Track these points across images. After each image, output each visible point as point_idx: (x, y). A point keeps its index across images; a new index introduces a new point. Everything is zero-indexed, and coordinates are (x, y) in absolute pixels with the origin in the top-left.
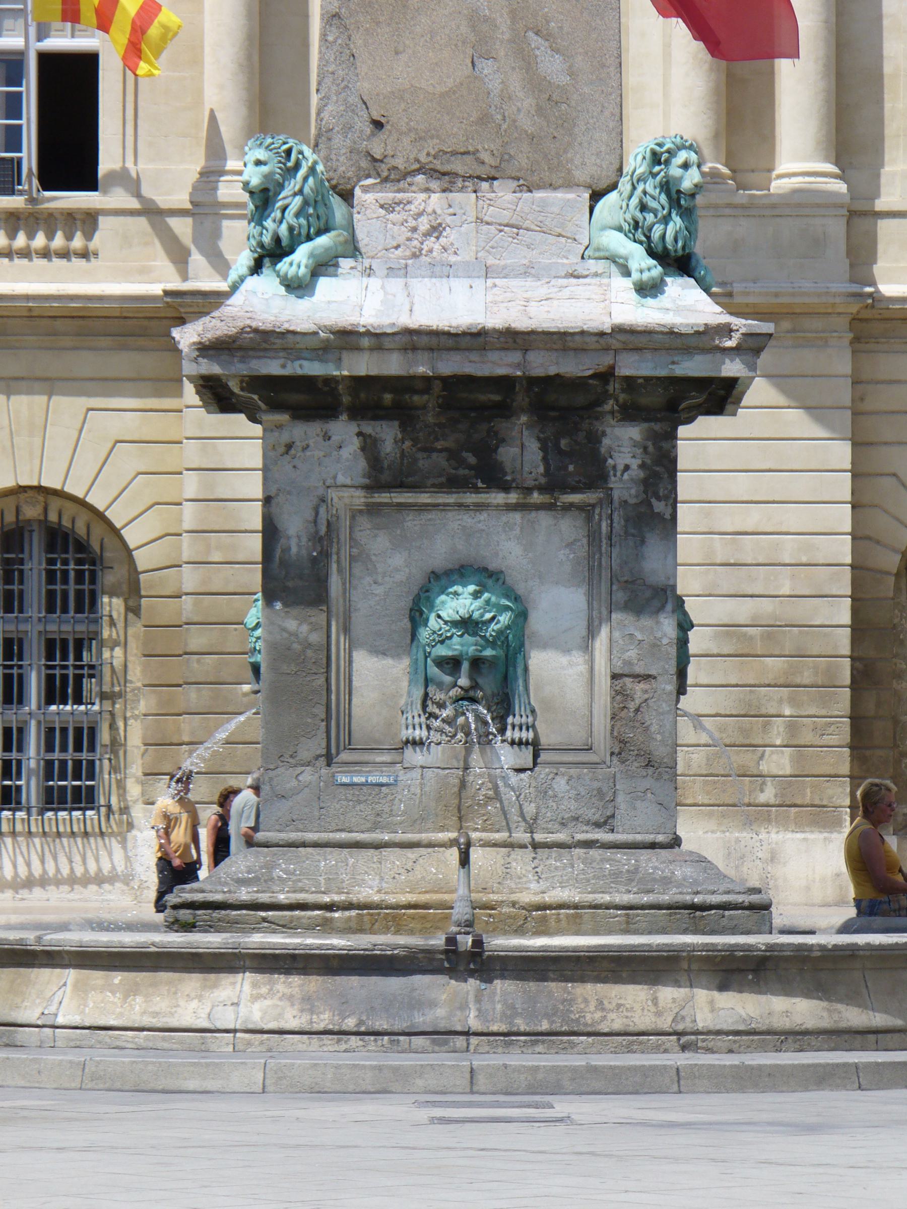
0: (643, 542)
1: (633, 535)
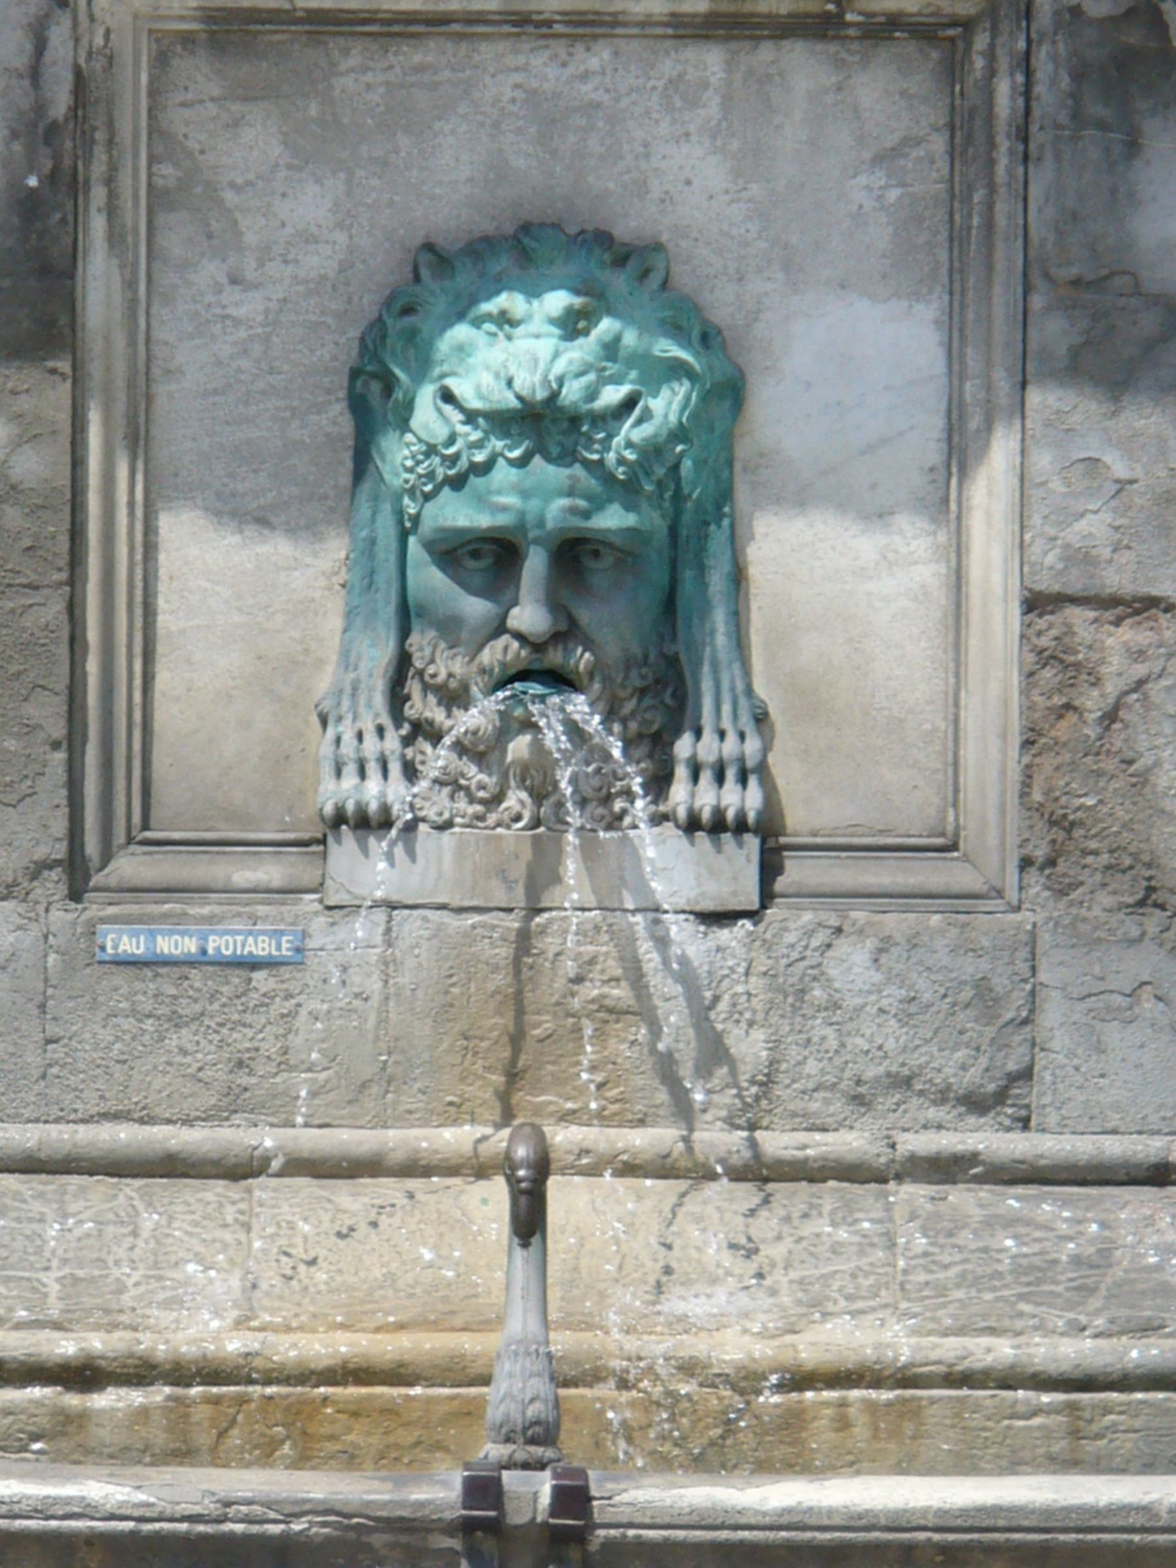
0: (1133, 146)
1: (1103, 126)
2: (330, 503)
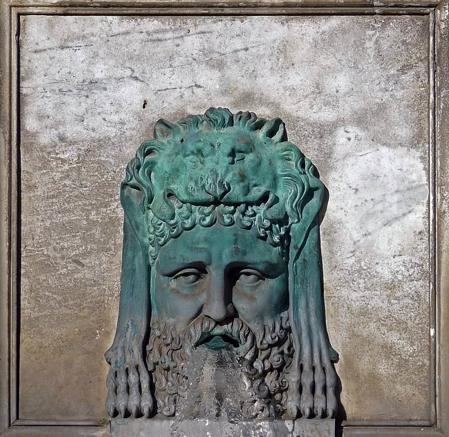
2: (111, 252)
